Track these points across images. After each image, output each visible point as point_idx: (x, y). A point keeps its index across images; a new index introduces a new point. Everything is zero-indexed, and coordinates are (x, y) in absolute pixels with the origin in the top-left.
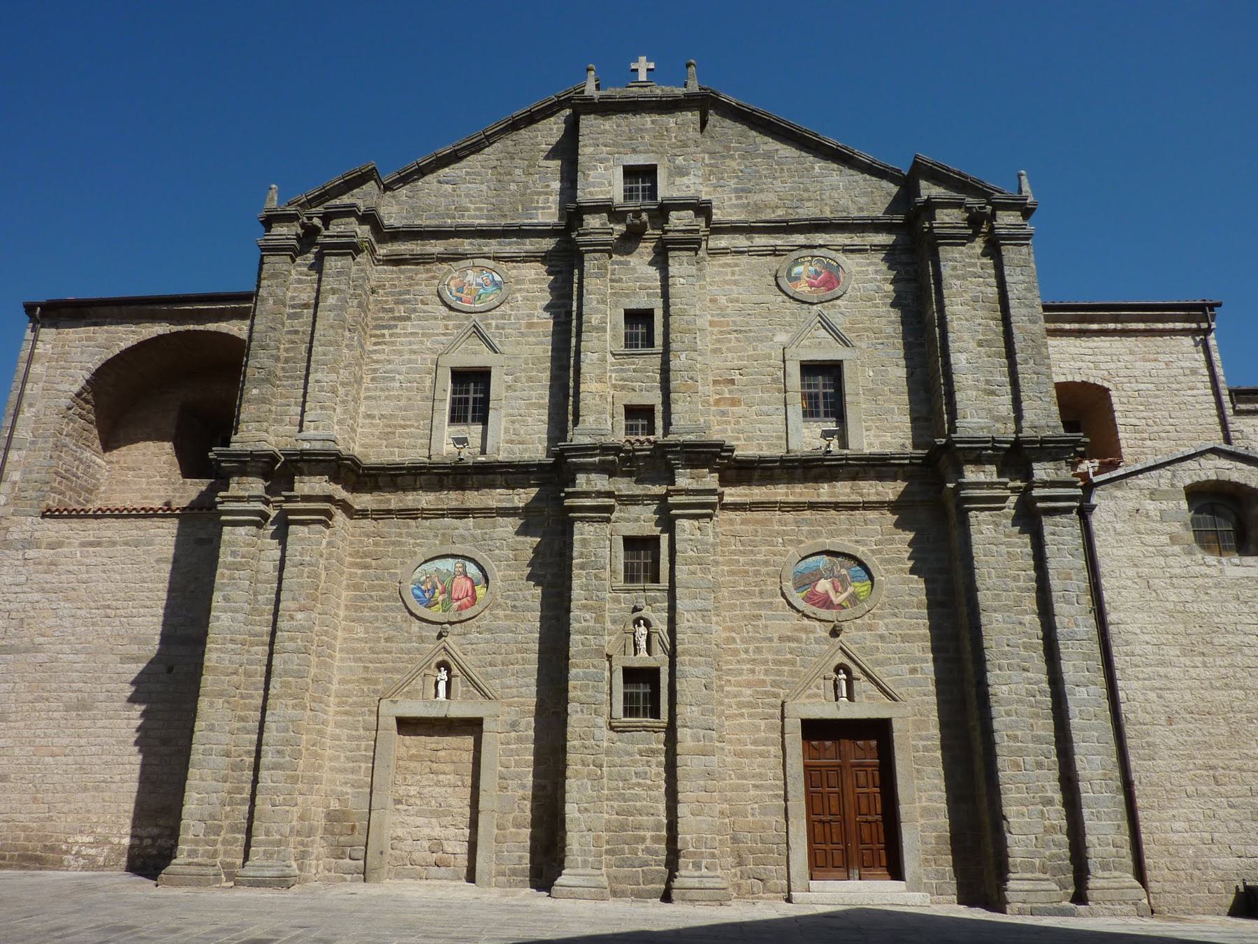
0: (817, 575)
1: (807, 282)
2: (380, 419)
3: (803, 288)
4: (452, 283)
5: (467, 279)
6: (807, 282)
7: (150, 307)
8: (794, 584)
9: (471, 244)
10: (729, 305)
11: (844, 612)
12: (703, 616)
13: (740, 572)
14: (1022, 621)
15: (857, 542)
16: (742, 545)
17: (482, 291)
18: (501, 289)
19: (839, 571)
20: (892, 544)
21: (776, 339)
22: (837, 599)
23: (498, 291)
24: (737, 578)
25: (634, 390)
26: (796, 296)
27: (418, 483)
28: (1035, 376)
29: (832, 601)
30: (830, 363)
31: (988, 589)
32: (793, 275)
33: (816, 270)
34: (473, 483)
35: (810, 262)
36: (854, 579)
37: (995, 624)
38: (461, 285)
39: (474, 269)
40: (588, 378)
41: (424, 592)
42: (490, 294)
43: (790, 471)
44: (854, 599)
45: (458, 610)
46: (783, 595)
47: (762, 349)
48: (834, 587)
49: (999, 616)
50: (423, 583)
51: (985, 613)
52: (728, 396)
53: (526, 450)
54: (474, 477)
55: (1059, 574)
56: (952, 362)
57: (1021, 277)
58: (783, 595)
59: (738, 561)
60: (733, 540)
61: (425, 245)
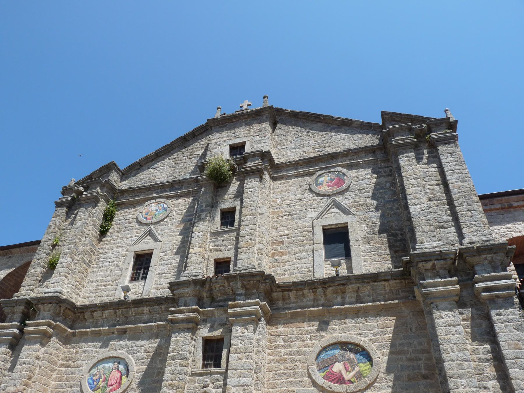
0: (334, 360)
1: (326, 185)
2: (95, 282)
3: (324, 189)
4: (144, 211)
5: (151, 208)
6: (326, 185)
7: (31, 247)
8: (318, 367)
10: (283, 202)
11: (352, 386)
12: (244, 390)
13: (281, 360)
14: (486, 386)
15: (361, 334)
16: (284, 341)
17: (157, 213)
18: (166, 211)
19: (349, 356)
20: (385, 335)
21: (308, 216)
22: (347, 376)
24: (279, 364)
25: (221, 251)
26: (320, 193)
27: (104, 315)
28: (469, 212)
29: (344, 378)
30: (341, 226)
31: (452, 360)
32: (318, 182)
33: (331, 179)
34: (132, 313)
35: (328, 175)
36: (359, 361)
37: (461, 389)
38: (148, 211)
39: (156, 204)
40: (194, 246)
41: (94, 381)
42: (161, 214)
43: (314, 290)
44: (360, 376)
46: (310, 376)
47: (300, 222)
48: (345, 368)
49: (463, 381)
50: (94, 375)
51: (452, 380)
52: (279, 250)
53: (164, 293)
54: (132, 309)
55: (509, 345)
56: (411, 211)
57: (452, 159)
58: (310, 376)
59: (280, 352)
60: (277, 338)
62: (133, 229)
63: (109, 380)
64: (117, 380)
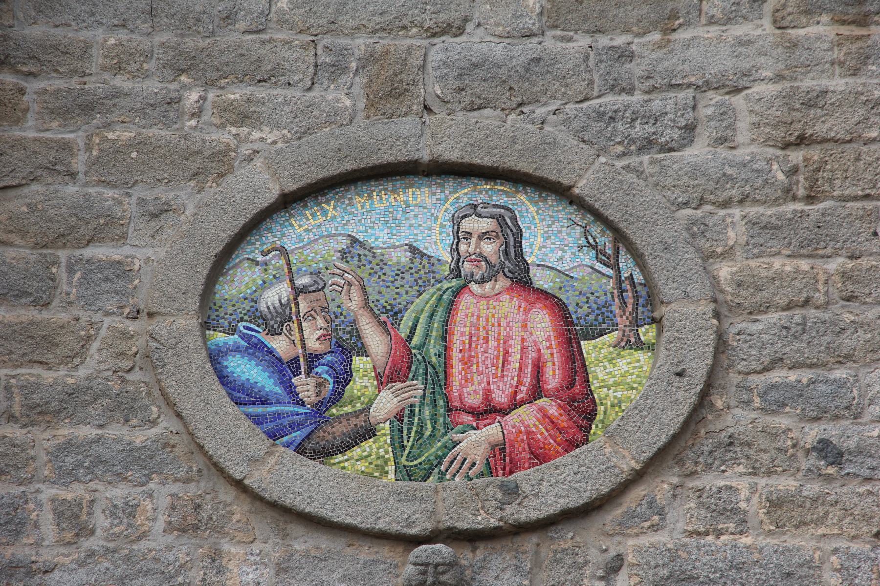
45: (490, 470)
63: (457, 368)
64: (538, 367)
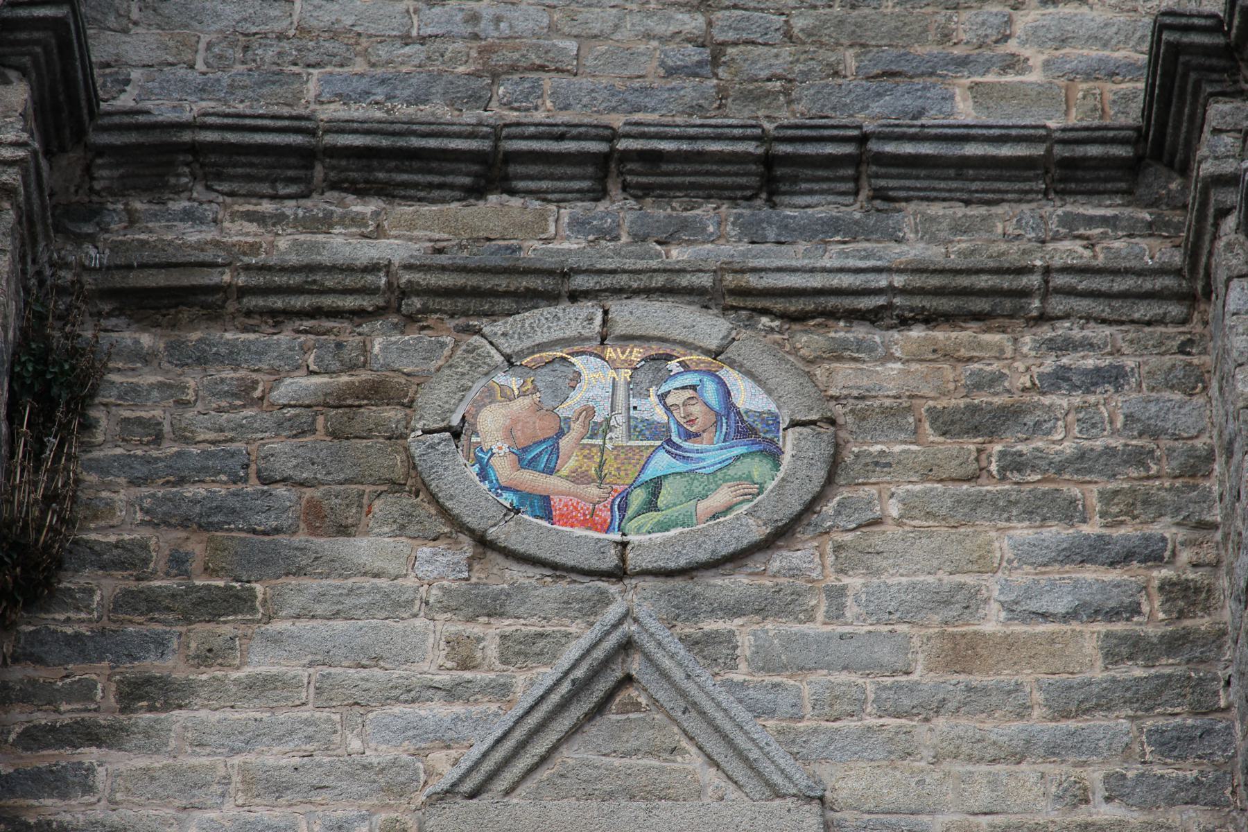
5: (577, 399)
9: (578, 225)
17: (662, 463)
23: (758, 468)
38: (545, 428)
42: (716, 477)
61: (325, 223)
62: (396, 605)
